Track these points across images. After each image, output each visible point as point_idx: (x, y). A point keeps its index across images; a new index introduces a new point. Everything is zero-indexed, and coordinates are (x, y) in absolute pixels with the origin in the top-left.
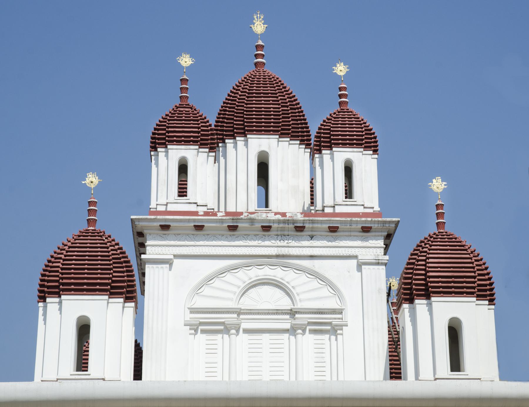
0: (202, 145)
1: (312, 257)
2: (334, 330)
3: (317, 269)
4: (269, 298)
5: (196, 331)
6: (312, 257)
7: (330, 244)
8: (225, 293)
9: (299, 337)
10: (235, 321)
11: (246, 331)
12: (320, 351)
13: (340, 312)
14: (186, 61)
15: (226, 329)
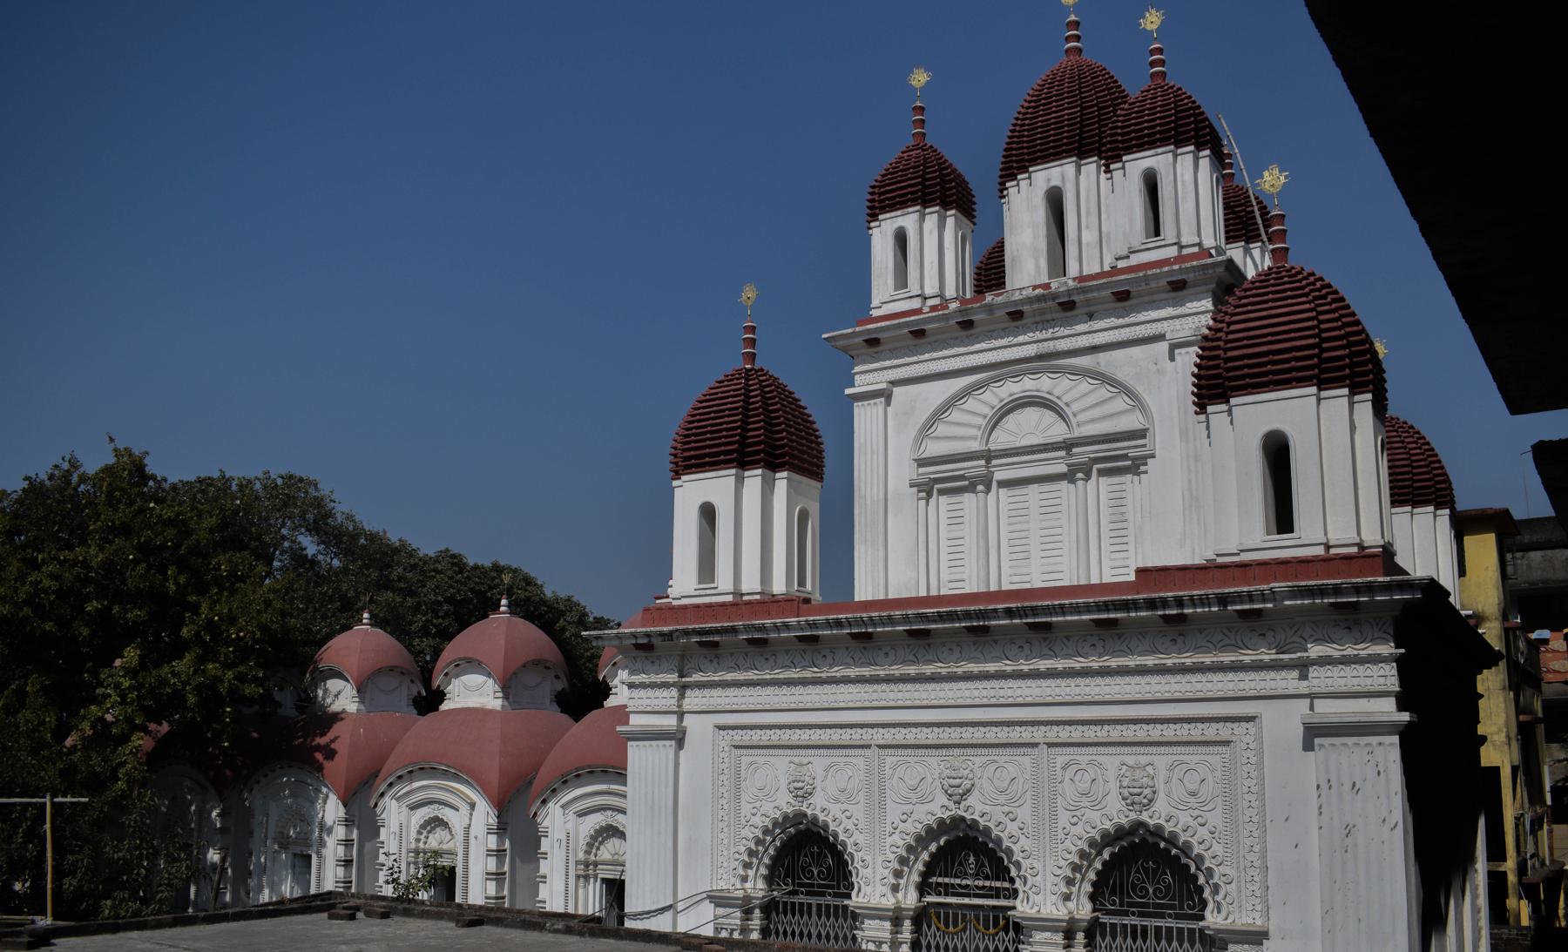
0: (926, 203)
1: (1095, 349)
2: (1136, 466)
3: (1103, 368)
4: (1030, 427)
5: (929, 495)
6: (1095, 349)
7: (1121, 321)
8: (963, 432)
9: (1080, 483)
10: (983, 471)
11: (1003, 484)
12: (1118, 502)
13: (1141, 434)
14: (920, 78)
15: (971, 485)
